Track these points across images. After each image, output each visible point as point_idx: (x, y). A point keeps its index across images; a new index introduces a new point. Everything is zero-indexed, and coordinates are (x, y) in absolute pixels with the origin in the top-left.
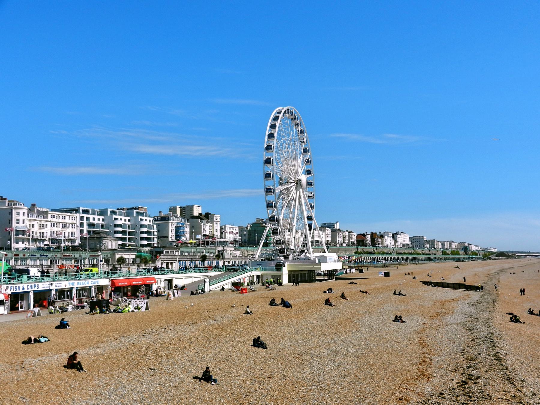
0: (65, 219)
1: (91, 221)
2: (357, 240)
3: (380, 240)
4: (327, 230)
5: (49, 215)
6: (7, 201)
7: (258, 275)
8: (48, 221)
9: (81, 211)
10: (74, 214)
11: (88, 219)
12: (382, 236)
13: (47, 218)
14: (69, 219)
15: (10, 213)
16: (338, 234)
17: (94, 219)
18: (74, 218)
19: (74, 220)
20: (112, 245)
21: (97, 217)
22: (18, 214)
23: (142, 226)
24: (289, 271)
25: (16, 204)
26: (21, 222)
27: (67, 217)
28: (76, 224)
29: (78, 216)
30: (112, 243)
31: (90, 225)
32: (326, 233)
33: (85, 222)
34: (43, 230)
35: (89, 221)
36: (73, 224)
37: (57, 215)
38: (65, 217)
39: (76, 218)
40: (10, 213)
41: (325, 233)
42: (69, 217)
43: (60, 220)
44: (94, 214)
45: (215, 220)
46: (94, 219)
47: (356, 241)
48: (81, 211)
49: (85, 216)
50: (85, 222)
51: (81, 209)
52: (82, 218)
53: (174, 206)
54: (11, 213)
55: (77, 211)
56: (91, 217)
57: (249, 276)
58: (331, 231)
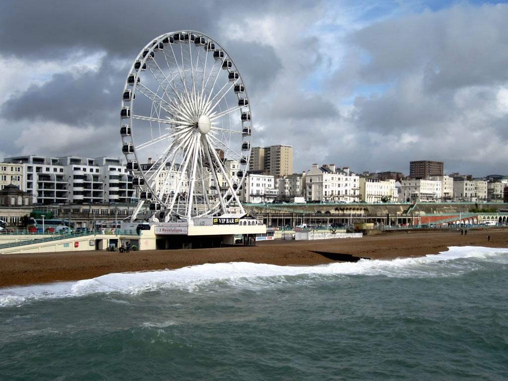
0: (5, 170)
1: (44, 172)
2: (505, 193)
4: (446, 179)
7: (110, 240)
14: (12, 170)
16: (466, 184)
17: (48, 169)
18: (19, 168)
19: (19, 171)
20: (23, 202)
21: (52, 167)
23: (113, 177)
24: (157, 235)
27: (9, 169)
28: (22, 176)
29: (25, 166)
30: (23, 198)
31: (41, 177)
32: (444, 183)
35: (42, 171)
36: (4, 175)
38: (5, 168)
39: (21, 169)
41: (442, 183)
42: (12, 168)
44: (49, 164)
45: (231, 167)
46: (48, 169)
47: (503, 194)
48: (31, 160)
49: (35, 166)
52: (30, 168)
55: (25, 160)
56: (44, 167)
57: (89, 240)
58: (454, 181)
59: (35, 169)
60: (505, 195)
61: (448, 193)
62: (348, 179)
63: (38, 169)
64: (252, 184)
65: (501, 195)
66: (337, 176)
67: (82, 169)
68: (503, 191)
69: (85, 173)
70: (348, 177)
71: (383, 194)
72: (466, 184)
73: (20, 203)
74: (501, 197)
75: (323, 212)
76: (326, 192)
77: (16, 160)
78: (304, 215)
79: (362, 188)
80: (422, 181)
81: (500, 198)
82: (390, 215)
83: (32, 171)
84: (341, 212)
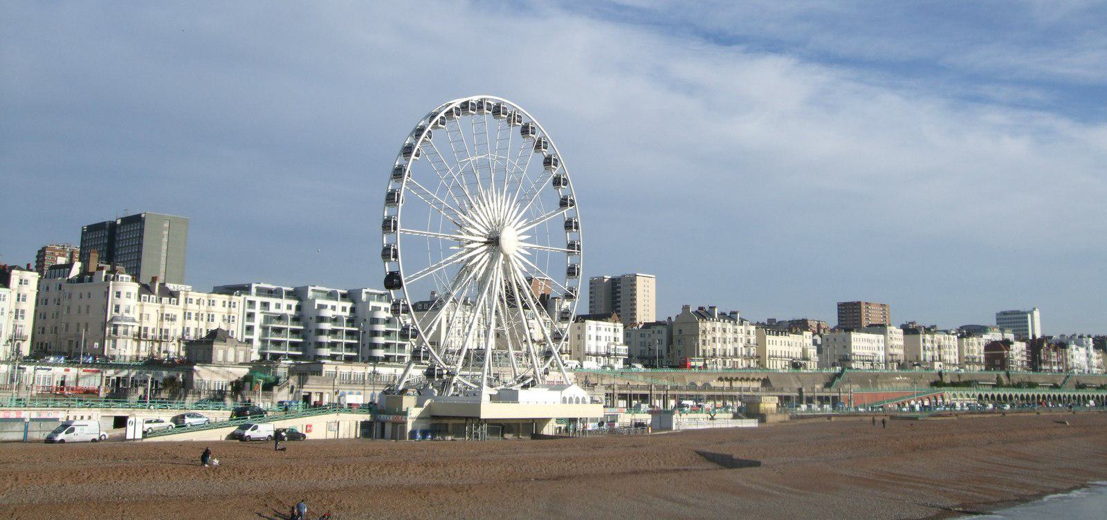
1: (273, 309)
3: (1055, 354)
5: (182, 298)
6: (104, 272)
8: (178, 308)
9: (254, 290)
10: (235, 298)
11: (265, 305)
12: (1062, 345)
13: (177, 304)
14: (224, 306)
15: (105, 292)
16: (924, 341)
17: (278, 306)
19: (234, 307)
20: (236, 356)
22: (118, 295)
25: (118, 276)
26: (122, 310)
30: (236, 352)
33: (257, 310)
34: (166, 325)
35: (269, 310)
37: (198, 298)
40: (105, 292)
42: (224, 302)
43: (203, 308)
46: (278, 306)
47: (983, 356)
49: (259, 300)
50: (257, 310)
51: (254, 286)
53: (630, 273)
54: (107, 294)
55: (245, 289)
56: (273, 301)
59: (258, 305)
60: (986, 358)
61: (896, 355)
62: (739, 331)
63: (265, 305)
64: (590, 336)
65: (980, 358)
66: (718, 325)
67: (329, 307)
68: (982, 351)
69: (335, 313)
70: (739, 328)
71: (794, 356)
72: (924, 341)
73: (231, 358)
74: (980, 360)
75: (699, 384)
76: (704, 351)
77: (229, 290)
78: (669, 388)
79: (761, 344)
80: (854, 335)
81: (979, 363)
82: (804, 390)
83: (254, 308)
84: (727, 384)
